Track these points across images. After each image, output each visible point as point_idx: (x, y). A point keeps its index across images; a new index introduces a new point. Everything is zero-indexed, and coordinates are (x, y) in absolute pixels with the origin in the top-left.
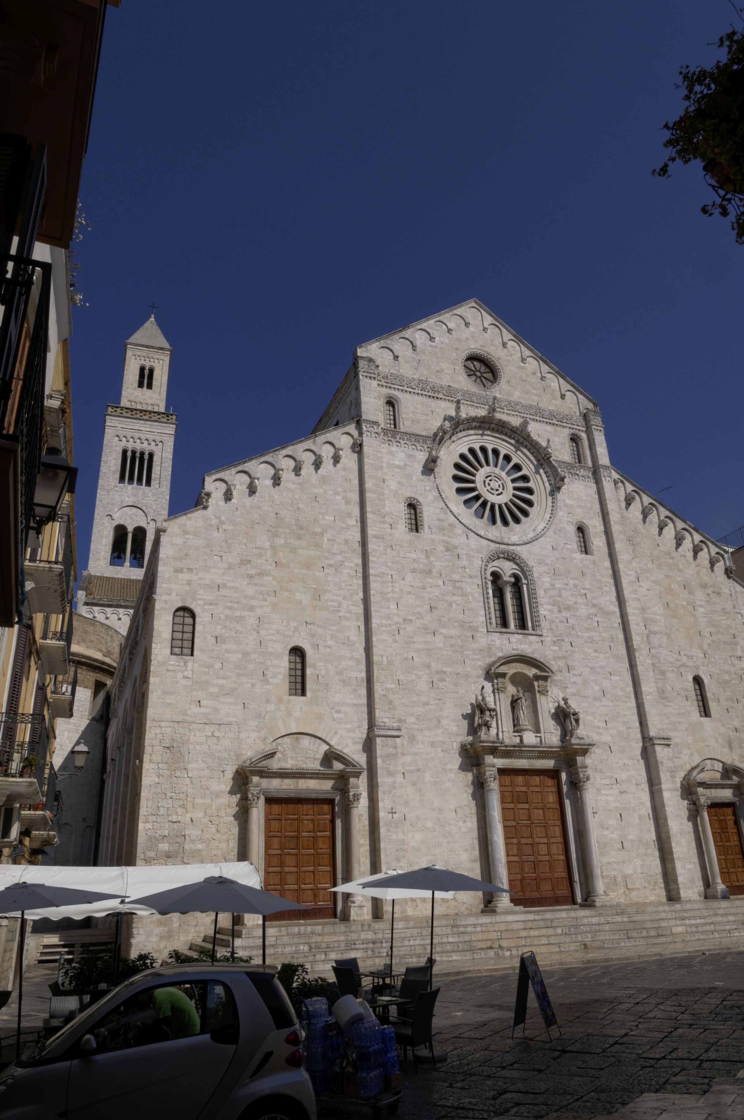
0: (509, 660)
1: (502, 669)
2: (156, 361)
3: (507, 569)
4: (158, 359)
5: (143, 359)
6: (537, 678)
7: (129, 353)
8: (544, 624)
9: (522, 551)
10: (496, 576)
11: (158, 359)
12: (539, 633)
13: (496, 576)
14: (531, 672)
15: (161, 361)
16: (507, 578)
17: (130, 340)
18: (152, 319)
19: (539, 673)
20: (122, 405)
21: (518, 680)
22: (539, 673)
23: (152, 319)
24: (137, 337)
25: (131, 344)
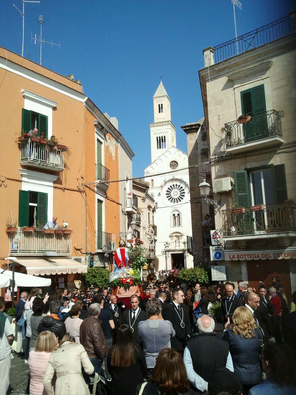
0: (174, 233)
1: (172, 235)
2: (163, 101)
3: (176, 213)
4: (163, 100)
5: (159, 102)
6: (180, 236)
7: (154, 101)
8: (183, 223)
9: (180, 209)
10: (174, 215)
11: (163, 100)
12: (182, 226)
13: (174, 215)
14: (179, 235)
15: (164, 101)
16: (176, 215)
17: (155, 96)
18: (161, 83)
19: (180, 235)
20: (155, 122)
21: (176, 236)
22: (180, 235)
23: (161, 83)
24: (157, 94)
25: (154, 98)
